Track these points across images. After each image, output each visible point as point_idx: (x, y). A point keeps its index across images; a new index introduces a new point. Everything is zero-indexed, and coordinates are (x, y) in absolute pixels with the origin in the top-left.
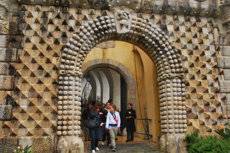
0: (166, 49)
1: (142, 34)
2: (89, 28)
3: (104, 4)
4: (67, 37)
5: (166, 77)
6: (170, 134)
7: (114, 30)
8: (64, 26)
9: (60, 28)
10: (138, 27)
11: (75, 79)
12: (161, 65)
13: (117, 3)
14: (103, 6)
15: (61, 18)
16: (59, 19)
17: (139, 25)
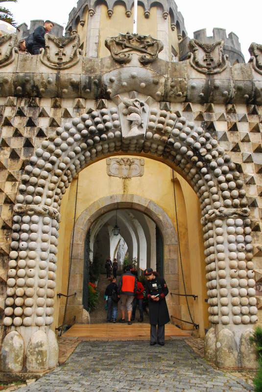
0: (214, 163)
1: (169, 138)
2: (73, 130)
3: (100, 89)
4: (33, 147)
5: (214, 215)
6: (224, 326)
7: (118, 133)
8: (29, 129)
9: (21, 131)
10: (161, 126)
11: (43, 221)
12: (206, 194)
13: (123, 86)
14: (97, 91)
15: (25, 116)
16: (22, 118)
17: (163, 123)
